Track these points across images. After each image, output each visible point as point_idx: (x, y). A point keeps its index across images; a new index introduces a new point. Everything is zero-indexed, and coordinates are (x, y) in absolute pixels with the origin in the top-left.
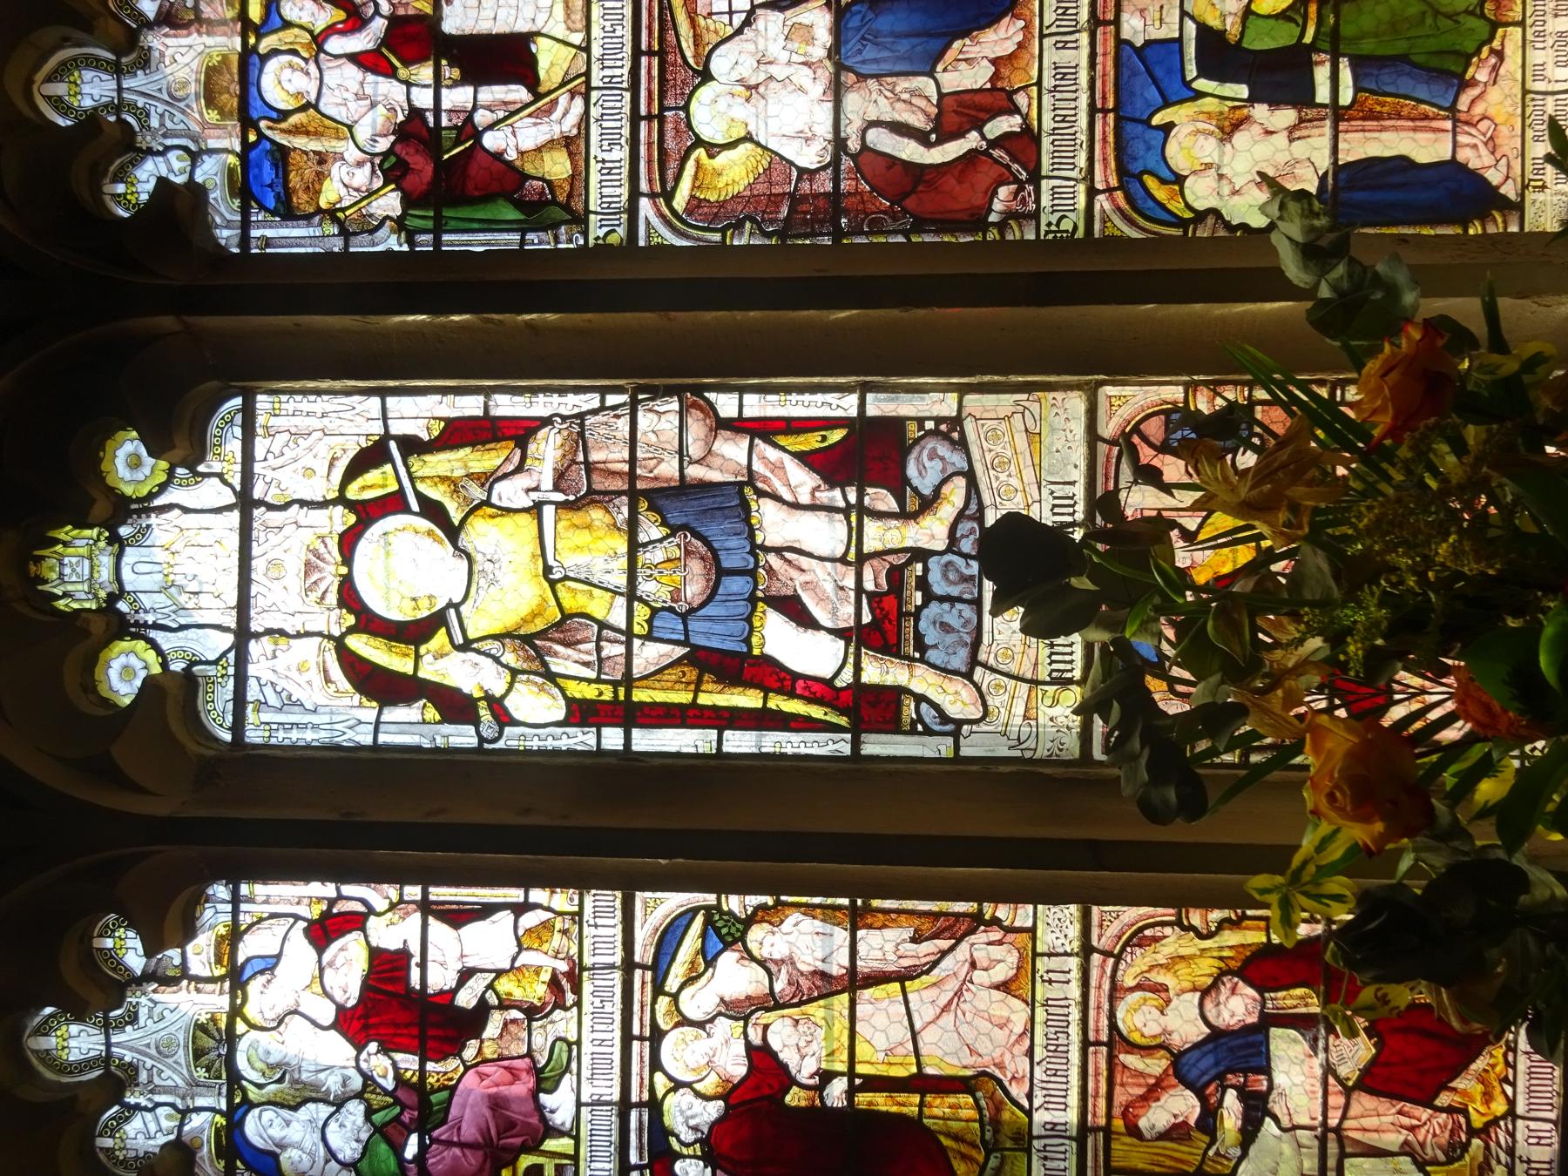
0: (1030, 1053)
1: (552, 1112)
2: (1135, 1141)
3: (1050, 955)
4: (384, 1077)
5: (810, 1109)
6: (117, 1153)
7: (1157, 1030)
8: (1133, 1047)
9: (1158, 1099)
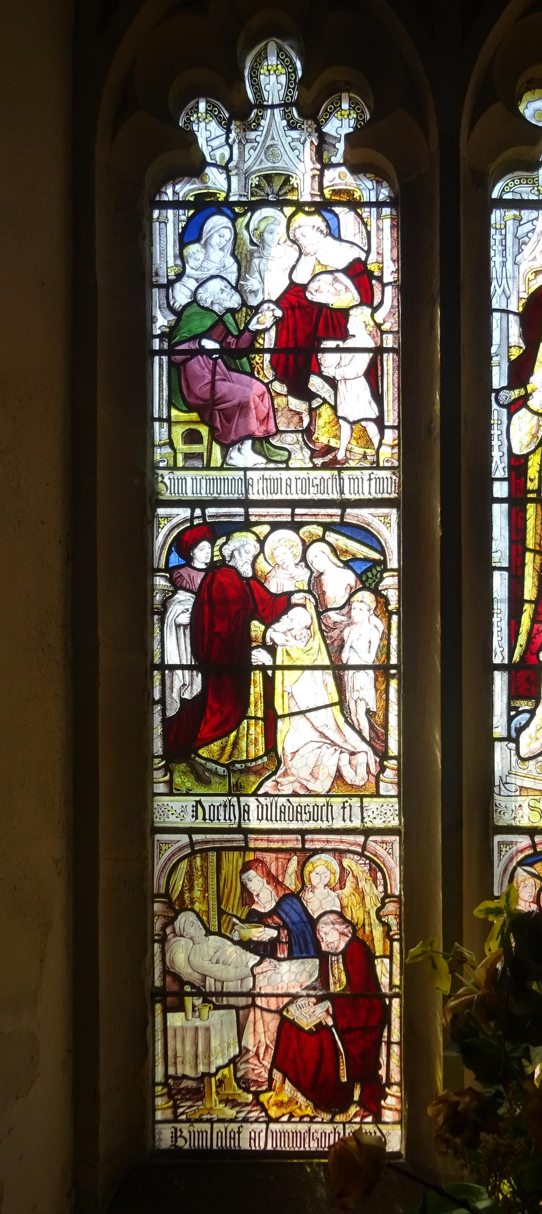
0: (295, 794)
1: (239, 450)
2: (240, 868)
3: (362, 807)
4: (258, 323)
5: (250, 640)
6: (195, 116)
8: (302, 865)
9: (268, 884)
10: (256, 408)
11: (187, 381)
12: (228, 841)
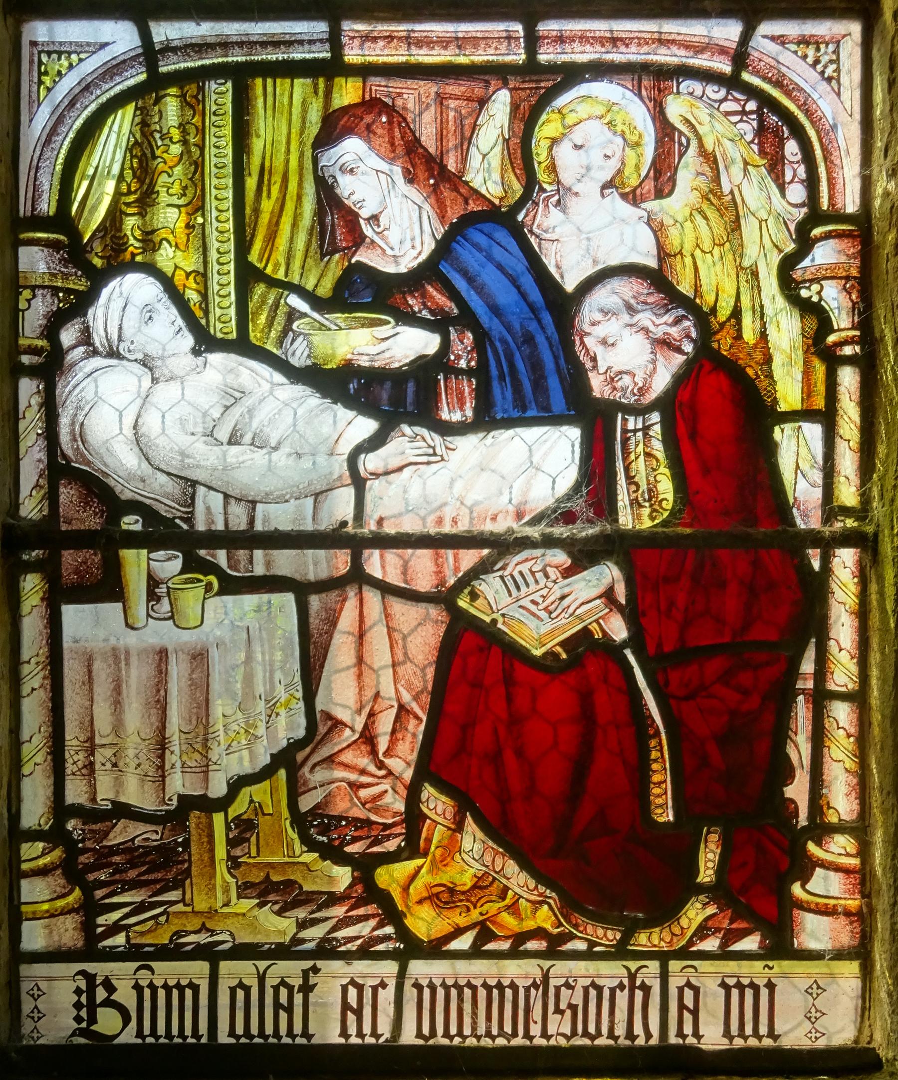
2: (314, 130)
7: (567, 177)
9: (411, 179)
12: (276, 43)
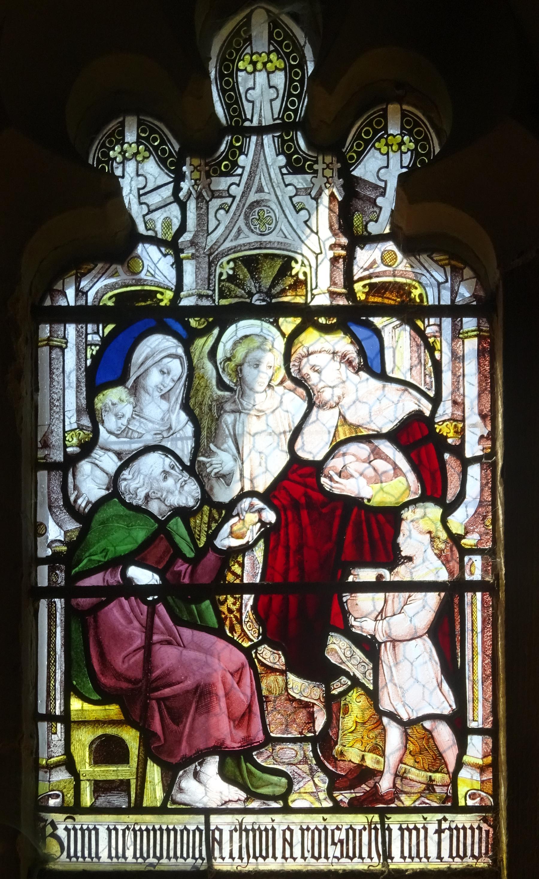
1: (196, 775)
4: (231, 534)
6: (118, 148)
10: (227, 695)
11: (99, 644)
